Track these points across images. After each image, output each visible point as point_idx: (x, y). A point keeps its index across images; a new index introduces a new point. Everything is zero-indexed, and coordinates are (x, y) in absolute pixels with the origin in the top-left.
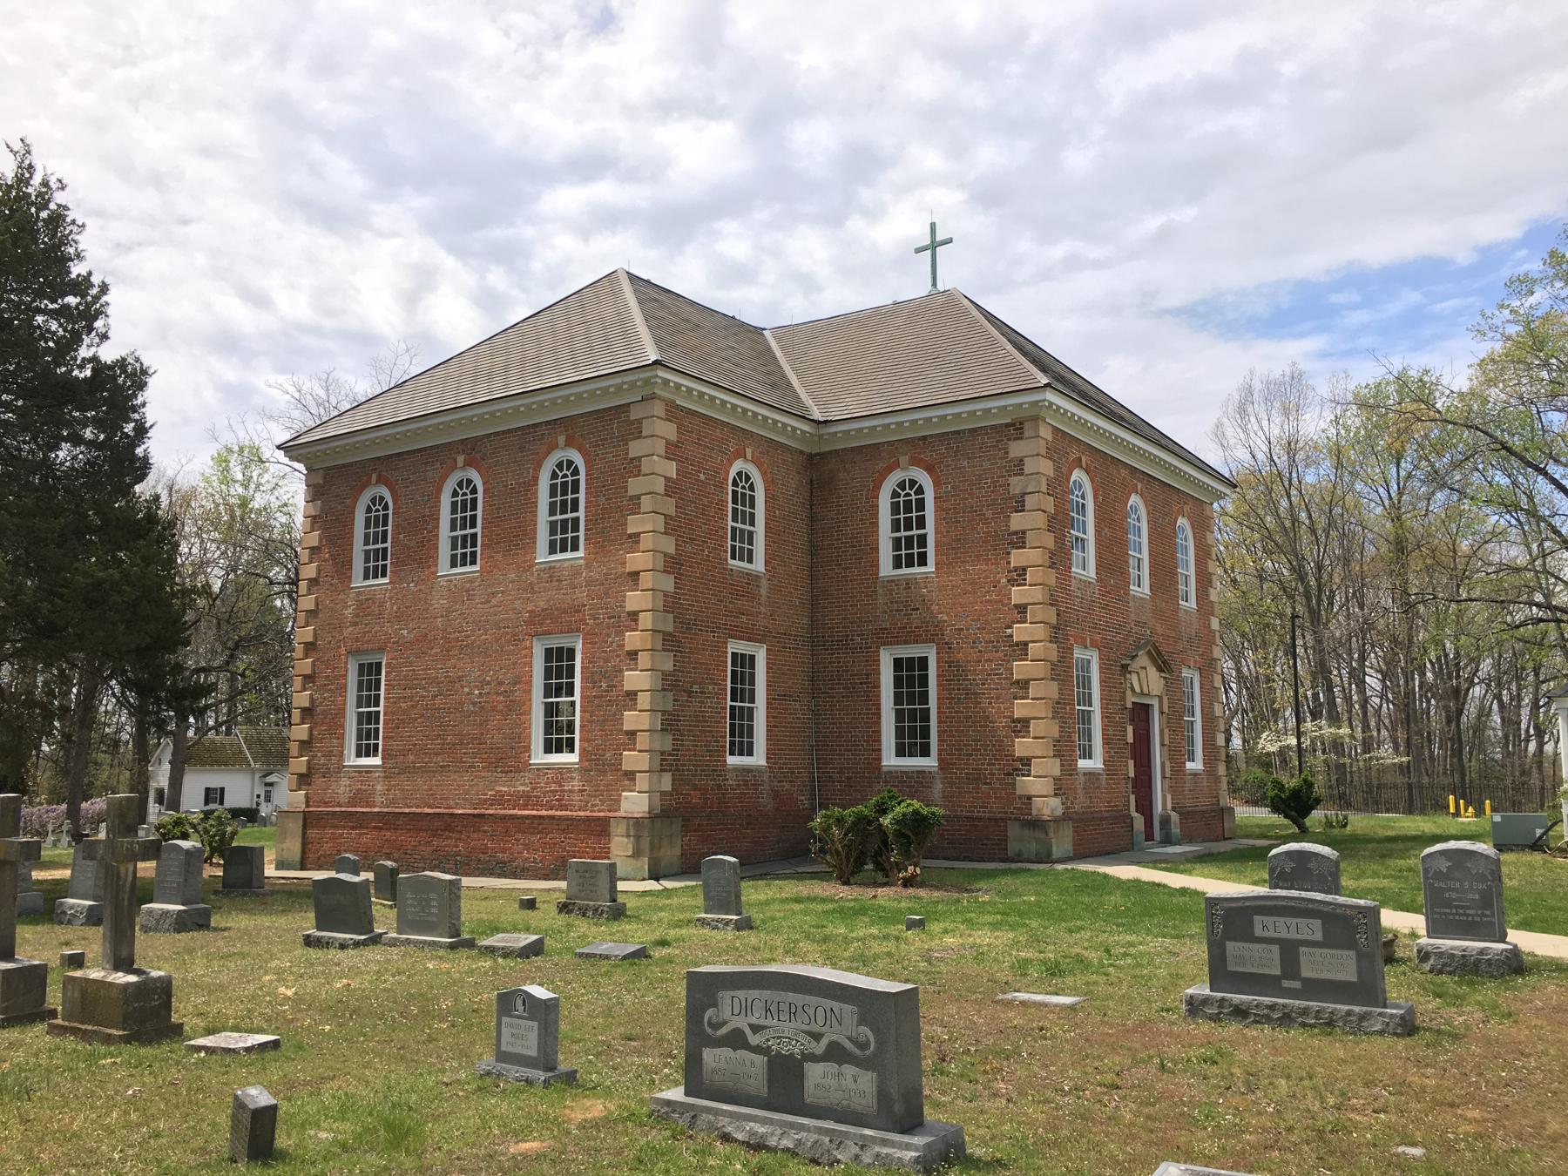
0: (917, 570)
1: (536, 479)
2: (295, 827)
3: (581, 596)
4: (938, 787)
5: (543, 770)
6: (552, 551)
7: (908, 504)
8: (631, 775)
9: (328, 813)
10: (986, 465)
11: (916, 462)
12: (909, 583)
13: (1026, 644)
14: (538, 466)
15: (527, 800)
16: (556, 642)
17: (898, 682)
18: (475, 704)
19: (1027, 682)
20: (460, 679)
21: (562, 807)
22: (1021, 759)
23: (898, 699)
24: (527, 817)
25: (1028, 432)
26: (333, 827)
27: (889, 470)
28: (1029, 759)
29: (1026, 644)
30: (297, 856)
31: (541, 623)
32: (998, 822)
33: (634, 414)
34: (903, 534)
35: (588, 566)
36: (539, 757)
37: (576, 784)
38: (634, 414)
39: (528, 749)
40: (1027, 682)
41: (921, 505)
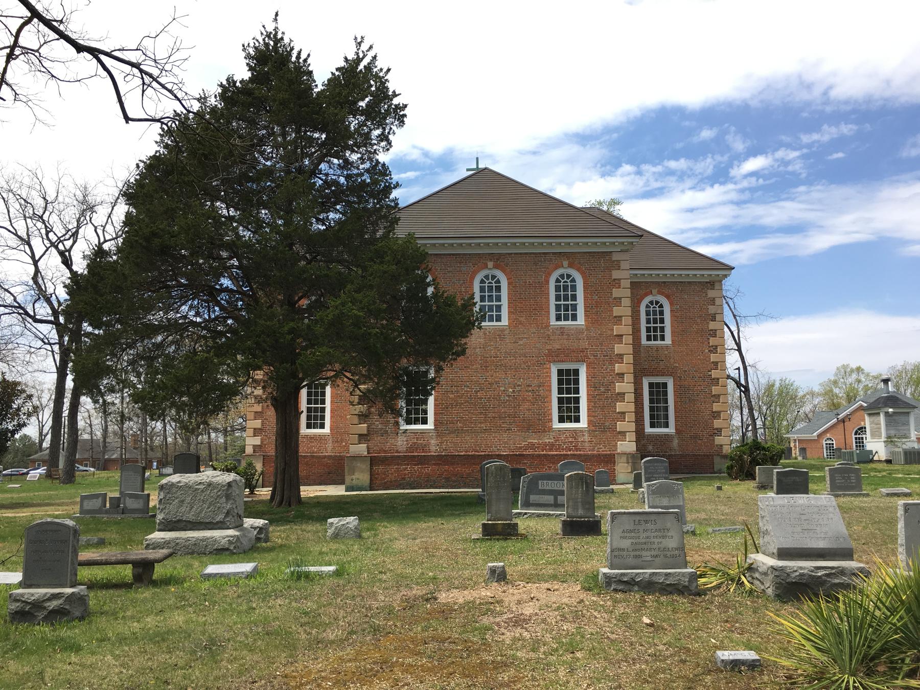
0: (659, 342)
1: (547, 282)
2: (366, 466)
3: (584, 344)
4: (676, 442)
5: (560, 431)
6: (558, 318)
7: (655, 313)
8: (623, 434)
9: (392, 457)
10: (697, 298)
11: (660, 293)
12: (658, 348)
13: (718, 379)
14: (550, 274)
15: (552, 446)
16: (565, 366)
17: (651, 393)
18: (509, 396)
19: (719, 396)
20: (497, 383)
21: (577, 450)
22: (717, 429)
23: (651, 401)
24: (556, 455)
25: (716, 287)
26: (398, 465)
27: (646, 295)
28: (721, 429)
29: (718, 379)
30: (368, 481)
31: (555, 356)
32: (709, 457)
33: (615, 257)
34: (652, 325)
35: (588, 329)
36: (557, 425)
37: (587, 438)
38: (615, 257)
39: (551, 420)
40: (719, 396)
41: (662, 313)
